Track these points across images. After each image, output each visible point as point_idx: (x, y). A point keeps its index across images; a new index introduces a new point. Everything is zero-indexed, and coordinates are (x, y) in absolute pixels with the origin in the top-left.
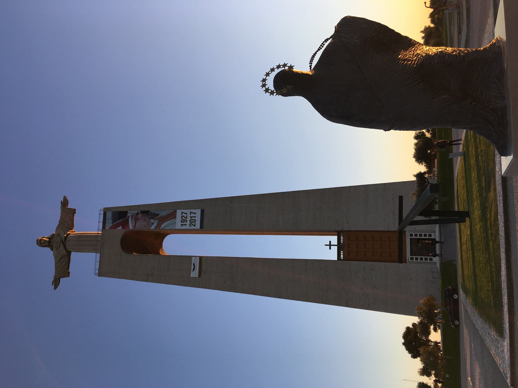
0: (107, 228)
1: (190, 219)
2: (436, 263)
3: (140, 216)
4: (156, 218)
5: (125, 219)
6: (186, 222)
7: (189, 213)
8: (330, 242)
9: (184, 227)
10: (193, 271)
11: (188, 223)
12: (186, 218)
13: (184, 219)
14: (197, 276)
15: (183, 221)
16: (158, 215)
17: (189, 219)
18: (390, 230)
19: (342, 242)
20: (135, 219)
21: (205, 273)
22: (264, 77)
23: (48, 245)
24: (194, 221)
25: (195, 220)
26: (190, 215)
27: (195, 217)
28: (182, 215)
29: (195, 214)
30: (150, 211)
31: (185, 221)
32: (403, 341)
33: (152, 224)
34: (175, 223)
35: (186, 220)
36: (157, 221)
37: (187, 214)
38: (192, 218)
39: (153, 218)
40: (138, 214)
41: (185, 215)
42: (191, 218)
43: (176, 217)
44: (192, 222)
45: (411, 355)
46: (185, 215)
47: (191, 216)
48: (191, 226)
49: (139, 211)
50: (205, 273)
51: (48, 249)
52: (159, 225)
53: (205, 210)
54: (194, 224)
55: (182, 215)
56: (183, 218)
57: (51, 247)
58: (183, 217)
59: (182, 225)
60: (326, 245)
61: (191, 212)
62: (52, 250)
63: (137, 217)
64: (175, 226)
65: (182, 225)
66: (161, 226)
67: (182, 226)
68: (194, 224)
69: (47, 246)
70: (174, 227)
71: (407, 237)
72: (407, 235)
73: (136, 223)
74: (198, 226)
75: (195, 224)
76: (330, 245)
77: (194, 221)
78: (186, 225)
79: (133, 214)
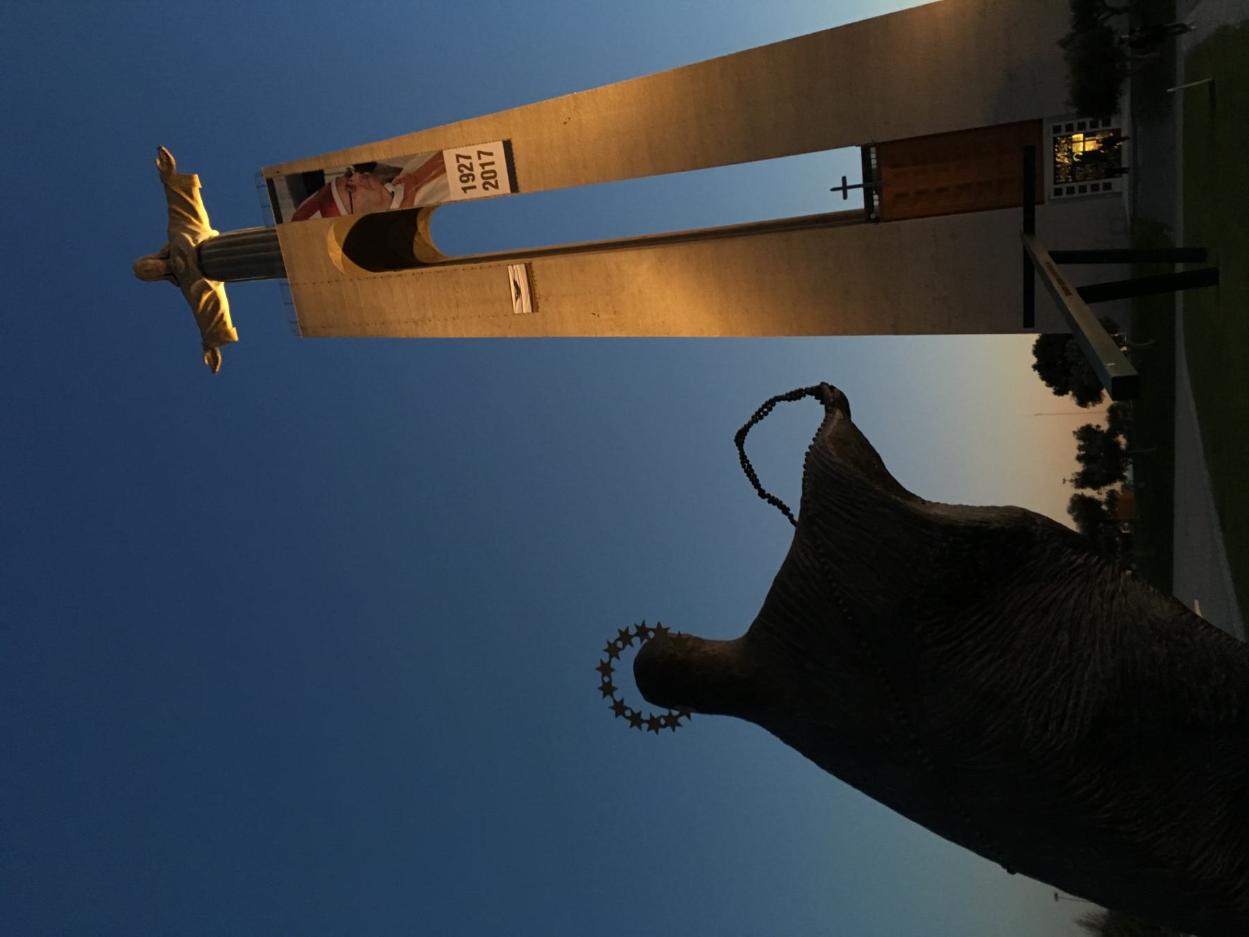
0: (287, 218)
1: (482, 170)
2: (1120, 194)
3: (356, 177)
4: (397, 178)
5: (323, 189)
6: (473, 180)
7: (475, 156)
8: (844, 179)
9: (471, 194)
10: (516, 299)
11: (479, 182)
12: (471, 169)
13: (466, 172)
14: (527, 308)
15: (465, 178)
16: (400, 170)
17: (478, 171)
18: (1001, 122)
19: (874, 167)
20: (346, 189)
22: (609, 701)
24: (492, 174)
25: (494, 172)
26: (480, 158)
27: (493, 163)
28: (458, 161)
29: (491, 154)
30: (379, 162)
31: (471, 178)
32: (1034, 360)
33: (390, 197)
34: (446, 186)
35: (473, 175)
36: (401, 187)
37: (469, 158)
38: (487, 168)
39: (390, 181)
40: (349, 174)
41: (467, 162)
42: (483, 168)
43: (444, 171)
44: (489, 179)
45: (1055, 389)
46: (467, 162)
47: (483, 161)
48: (487, 189)
49: (351, 167)
51: (167, 284)
52: (408, 197)
53: (513, 141)
54: (492, 181)
55: (458, 161)
56: (462, 171)
57: (172, 277)
58: (462, 168)
59: (465, 189)
60: (833, 190)
61: (479, 153)
62: (179, 285)
63: (350, 183)
64: (449, 194)
65: (465, 189)
66: (413, 200)
67: (465, 192)
68: (492, 181)
69: (166, 275)
70: (445, 197)
71: (1044, 136)
72: (1044, 131)
73: (353, 199)
74: (505, 187)
75: (496, 181)
76: (845, 188)
77: (492, 174)
78: (474, 187)
79: (339, 176)
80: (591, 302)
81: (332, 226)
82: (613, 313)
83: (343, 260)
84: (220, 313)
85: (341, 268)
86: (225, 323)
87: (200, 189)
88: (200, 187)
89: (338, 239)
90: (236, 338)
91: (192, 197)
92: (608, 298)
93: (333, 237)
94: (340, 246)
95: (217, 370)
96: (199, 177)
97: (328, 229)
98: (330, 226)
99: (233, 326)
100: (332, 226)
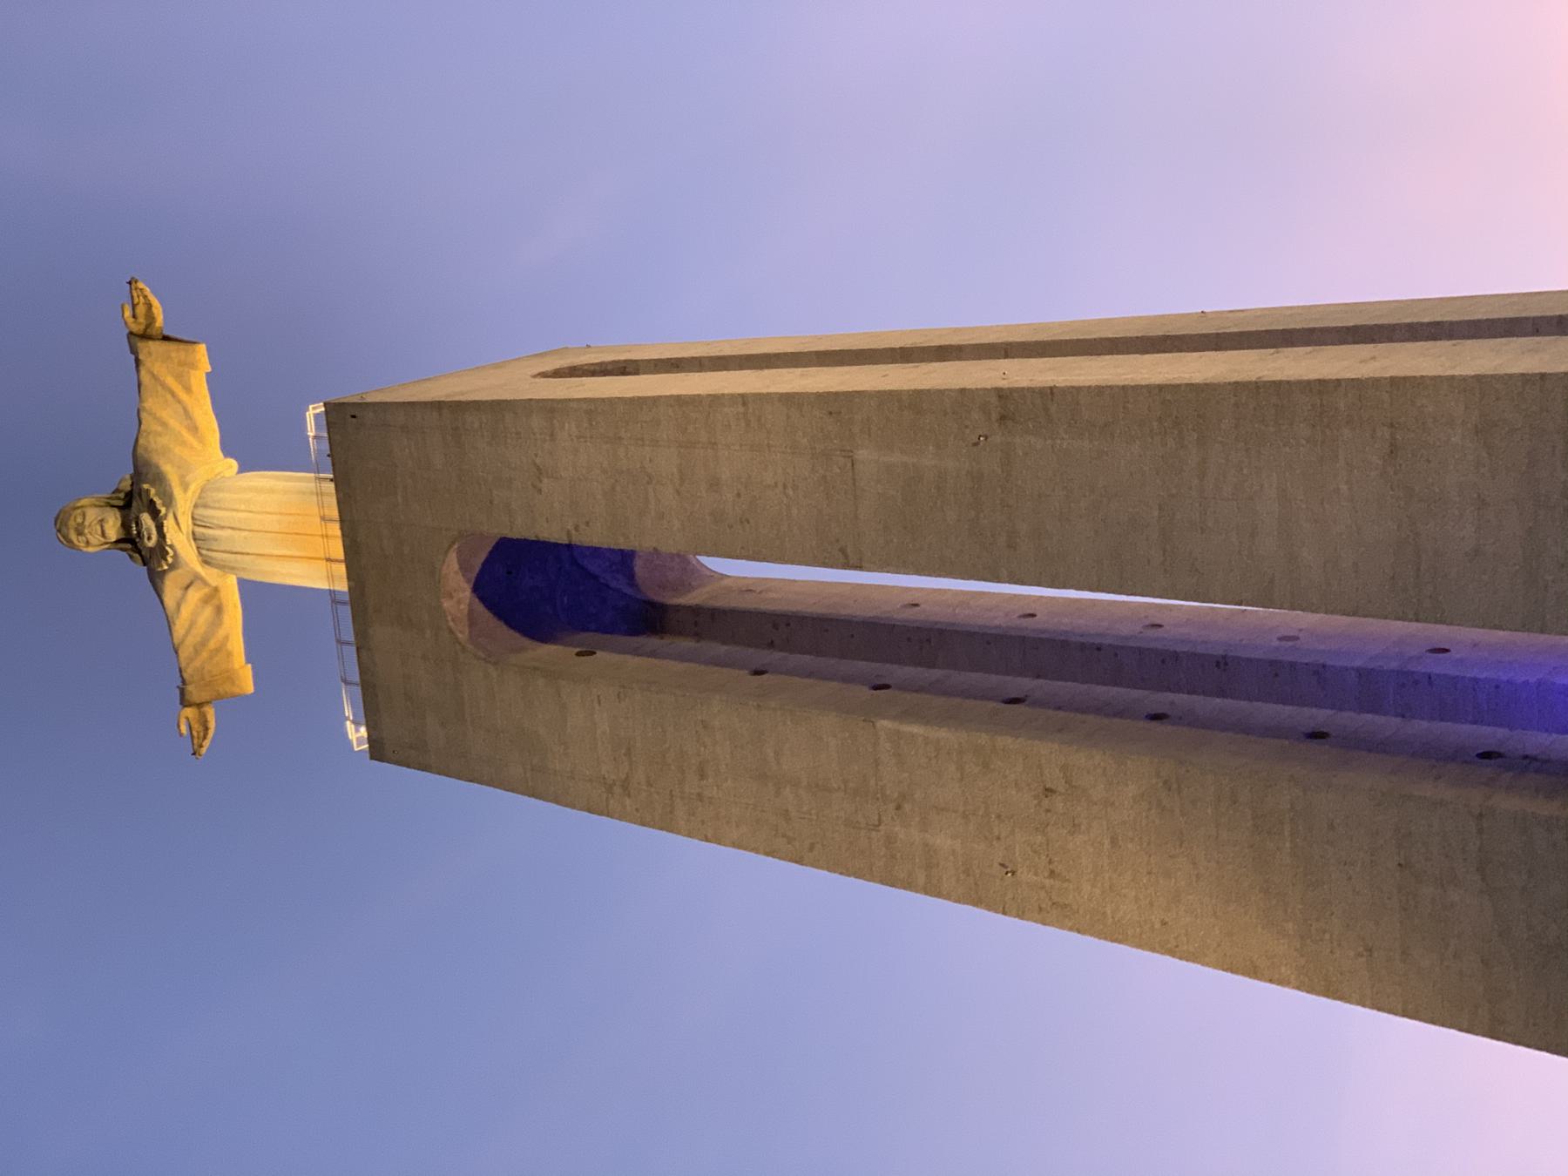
21: (898, 808)
23: (114, 540)
50: (898, 808)
57: (129, 546)
69: (118, 541)
80: (998, 838)
81: (456, 546)
82: (1046, 874)
83: (471, 611)
84: (221, 633)
85: (462, 637)
86: (229, 654)
87: (207, 374)
88: (209, 370)
89: (464, 567)
90: (249, 688)
91: (188, 389)
92: (1039, 838)
93: (456, 566)
94: (468, 581)
95: (204, 750)
96: (208, 350)
97: (446, 552)
98: (450, 547)
99: (248, 661)
100: (456, 546)
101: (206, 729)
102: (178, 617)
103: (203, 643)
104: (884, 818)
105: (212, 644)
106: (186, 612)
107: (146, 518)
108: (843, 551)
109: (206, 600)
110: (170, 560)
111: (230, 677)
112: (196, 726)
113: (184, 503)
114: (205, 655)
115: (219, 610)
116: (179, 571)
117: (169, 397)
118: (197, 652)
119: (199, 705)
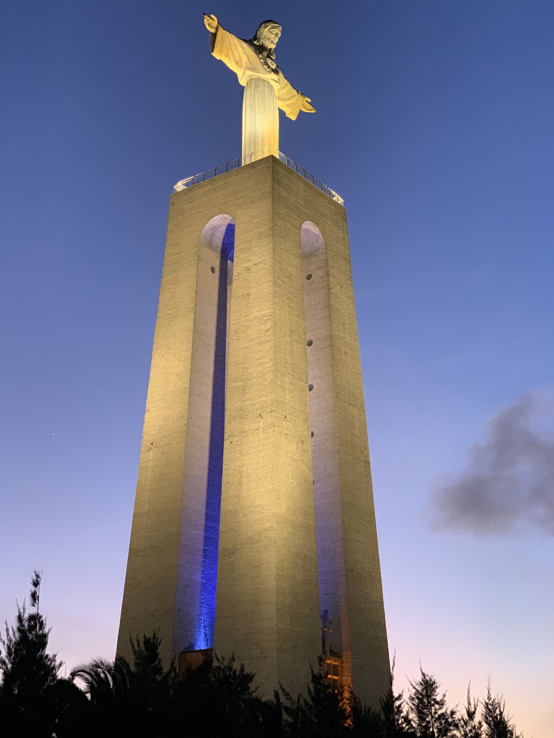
84: (232, 59)
86: (226, 56)
91: (288, 106)
99: (220, 60)
101: (209, 25)
102: (240, 44)
103: (231, 48)
104: (289, 375)
105: (230, 52)
106: (240, 48)
107: (274, 67)
108: (338, 393)
109: (240, 58)
110: (266, 67)
111: (221, 51)
112: (211, 20)
113: (276, 86)
114: (228, 46)
115: (237, 63)
116: (260, 66)
117: (288, 96)
118: (230, 43)
119: (217, 29)
